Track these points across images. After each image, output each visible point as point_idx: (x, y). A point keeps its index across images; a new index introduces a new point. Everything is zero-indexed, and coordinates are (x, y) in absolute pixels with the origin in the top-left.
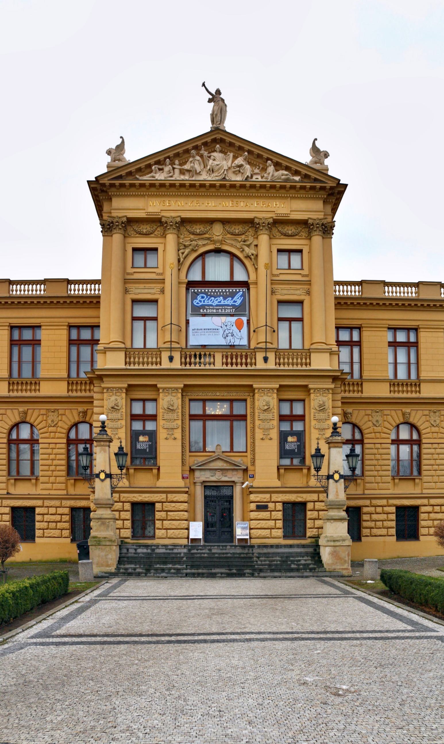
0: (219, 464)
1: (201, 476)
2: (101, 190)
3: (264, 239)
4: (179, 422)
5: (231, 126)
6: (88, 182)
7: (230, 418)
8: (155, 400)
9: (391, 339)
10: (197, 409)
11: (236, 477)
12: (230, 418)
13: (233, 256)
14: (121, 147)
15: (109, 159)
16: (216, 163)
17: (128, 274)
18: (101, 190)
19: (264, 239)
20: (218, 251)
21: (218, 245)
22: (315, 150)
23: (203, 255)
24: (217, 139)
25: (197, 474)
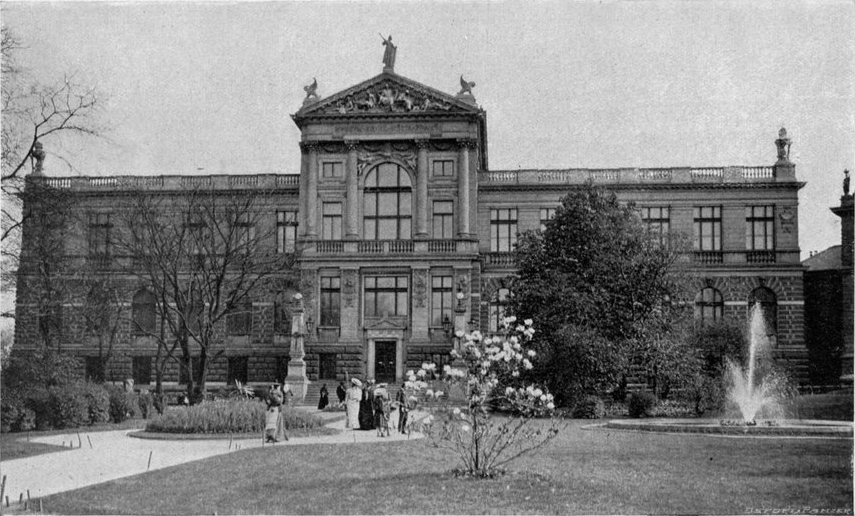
0: (385, 325)
1: (373, 334)
2: (301, 121)
3: (424, 154)
4: (357, 295)
5: (401, 69)
6: (292, 116)
7: (396, 290)
8: (339, 277)
9: (749, 215)
10: (371, 282)
11: (398, 335)
12: (396, 290)
13: (399, 166)
14: (315, 85)
15: (305, 94)
16: (385, 99)
17: (320, 183)
18: (301, 121)
19: (424, 154)
20: (389, 163)
21: (388, 160)
22: (463, 83)
23: (377, 166)
24: (388, 80)
25: (369, 332)
